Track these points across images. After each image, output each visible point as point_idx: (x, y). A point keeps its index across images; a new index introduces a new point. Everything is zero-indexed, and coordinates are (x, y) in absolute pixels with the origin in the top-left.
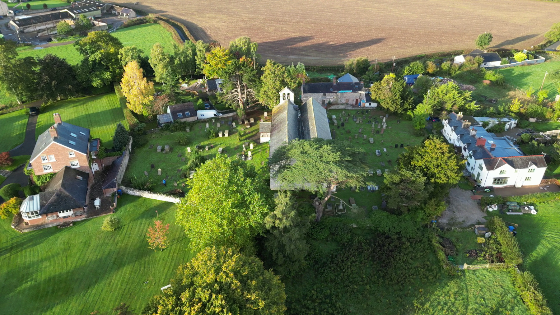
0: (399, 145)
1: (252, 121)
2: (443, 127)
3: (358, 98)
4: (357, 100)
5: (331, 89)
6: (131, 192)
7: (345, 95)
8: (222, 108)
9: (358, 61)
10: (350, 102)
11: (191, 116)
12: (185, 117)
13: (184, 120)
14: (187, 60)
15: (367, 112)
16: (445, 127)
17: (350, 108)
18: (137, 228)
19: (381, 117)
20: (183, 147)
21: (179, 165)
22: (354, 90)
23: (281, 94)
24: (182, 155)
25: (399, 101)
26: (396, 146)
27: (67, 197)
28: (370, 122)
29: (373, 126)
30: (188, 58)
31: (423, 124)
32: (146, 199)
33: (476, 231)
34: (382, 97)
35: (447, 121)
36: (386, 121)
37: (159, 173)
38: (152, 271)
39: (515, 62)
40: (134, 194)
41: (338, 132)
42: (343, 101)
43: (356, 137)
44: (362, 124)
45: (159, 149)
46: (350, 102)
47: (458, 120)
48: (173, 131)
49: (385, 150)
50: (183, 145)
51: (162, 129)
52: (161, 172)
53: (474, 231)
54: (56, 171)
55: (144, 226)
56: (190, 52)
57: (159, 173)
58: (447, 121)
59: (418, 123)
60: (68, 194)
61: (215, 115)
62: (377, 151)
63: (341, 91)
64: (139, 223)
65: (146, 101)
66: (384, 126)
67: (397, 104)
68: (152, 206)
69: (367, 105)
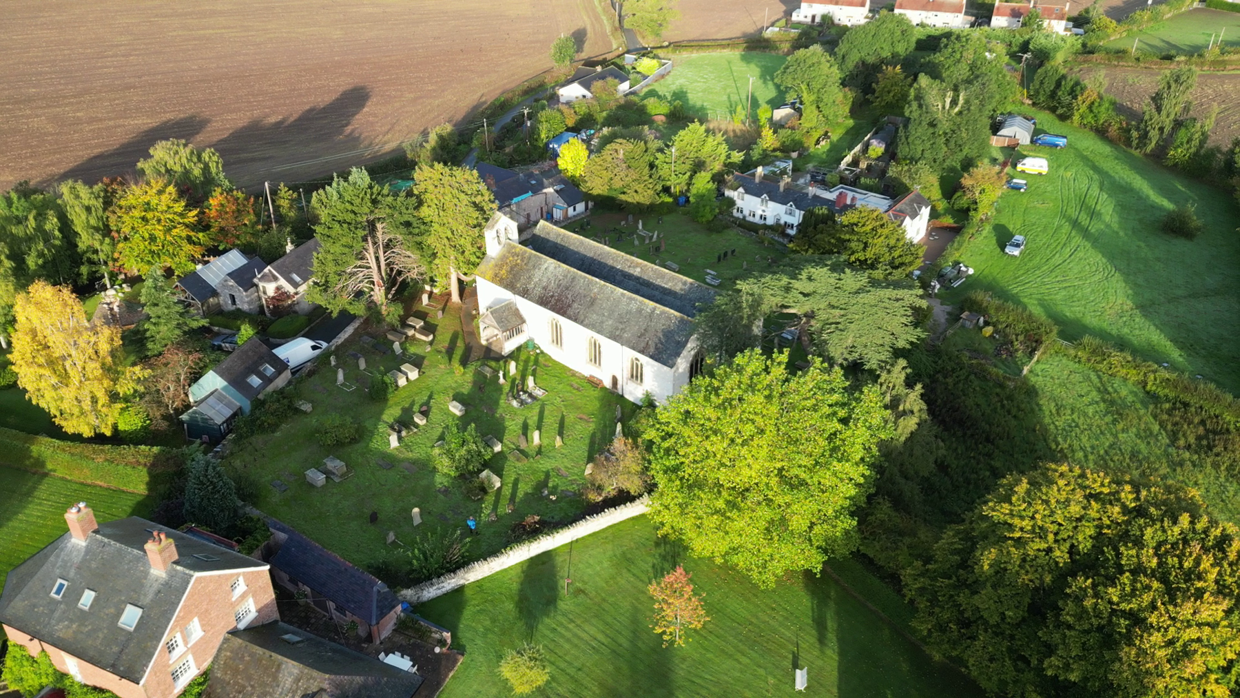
1: (419, 324)
6: (431, 592)
7: (524, 205)
8: (318, 323)
11: (279, 373)
12: (268, 380)
13: (270, 388)
14: (54, 246)
16: (739, 203)
18: (561, 641)
20: (358, 447)
21: (424, 482)
24: (389, 462)
27: (364, 686)
30: (57, 242)
32: (479, 584)
33: (968, 323)
34: (617, 184)
37: (417, 520)
38: (727, 682)
39: (645, 77)
40: (439, 592)
45: (320, 479)
47: (761, 183)
48: (274, 427)
50: (354, 441)
51: (240, 437)
52: (421, 514)
53: (963, 326)
54: (205, 665)
55: (567, 629)
56: (52, 223)
57: (417, 520)
58: (741, 190)
60: (359, 679)
61: (314, 348)
63: (515, 200)
64: (547, 633)
65: (125, 388)
68: (515, 586)
69: (570, 211)
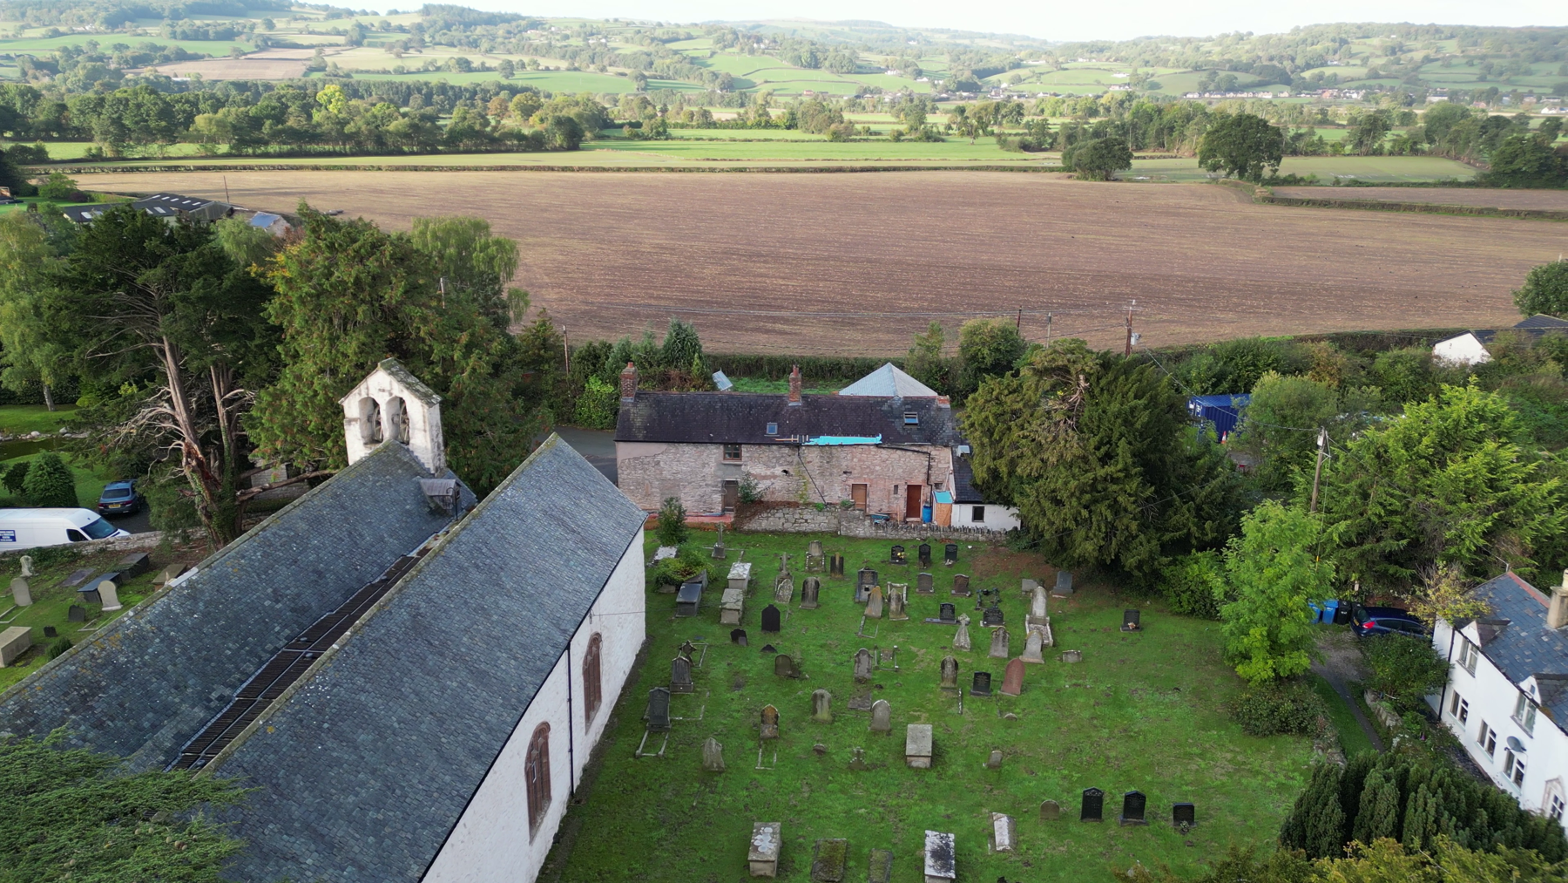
0: (1114, 803)
2: (1440, 673)
3: (918, 479)
4: (913, 491)
5: (772, 429)
9: (973, 332)
10: (878, 501)
15: (951, 553)
16: (1459, 676)
17: (863, 530)
19: (1027, 584)
22: (893, 440)
23: (352, 406)
25: (1131, 493)
26: (1092, 807)
28: (948, 613)
29: (963, 639)
31: (1296, 644)
35: (1472, 631)
36: (1049, 608)
41: (719, 670)
42: (837, 492)
43: (823, 713)
44: (898, 626)
46: (878, 501)
49: (1002, 828)
58: (1472, 631)
59: (1257, 632)
62: (932, 839)
63: (824, 440)
66: (1034, 646)
67: (1116, 508)
69: (962, 516)
